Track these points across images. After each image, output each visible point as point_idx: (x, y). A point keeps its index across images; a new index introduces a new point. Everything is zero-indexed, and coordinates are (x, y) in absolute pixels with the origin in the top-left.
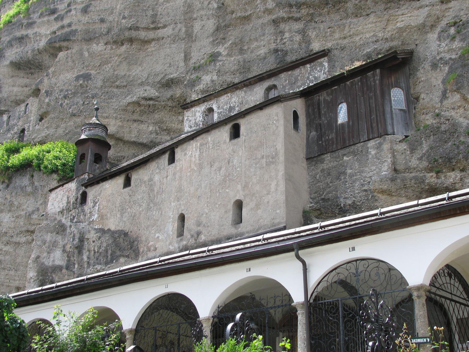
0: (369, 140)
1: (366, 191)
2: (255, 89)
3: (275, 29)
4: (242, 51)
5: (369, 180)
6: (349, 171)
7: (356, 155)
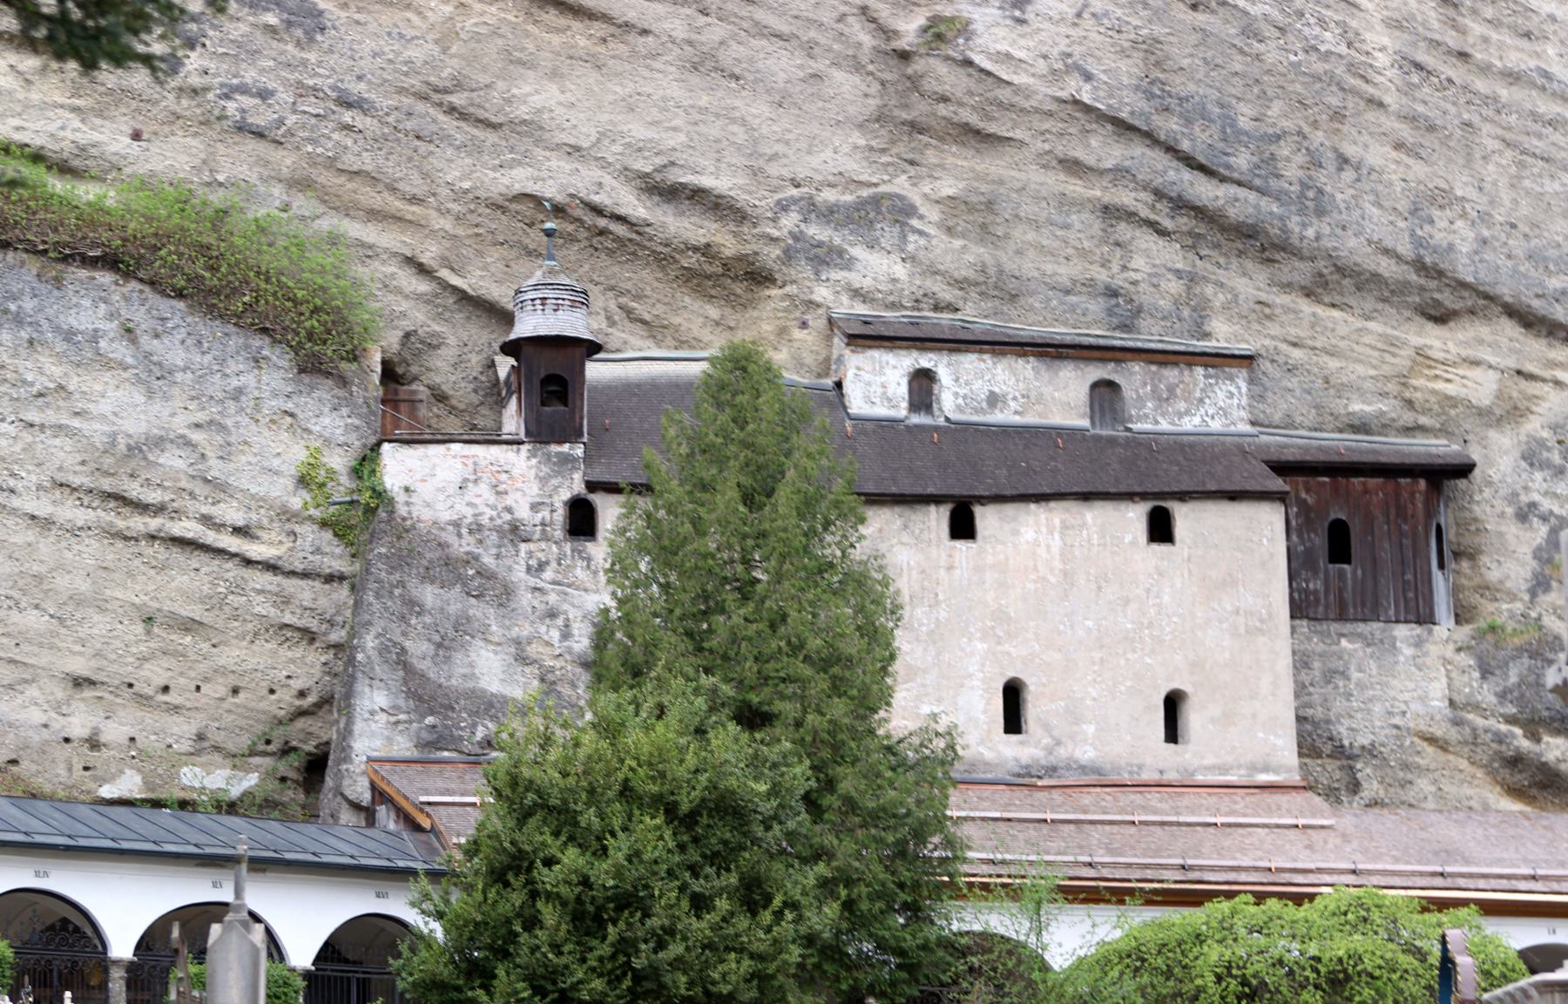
0: (1397, 621)
1: (1397, 727)
2: (1061, 374)
3: (1104, 230)
4: (985, 233)
5: (1404, 708)
6: (1355, 675)
7: (1369, 645)
